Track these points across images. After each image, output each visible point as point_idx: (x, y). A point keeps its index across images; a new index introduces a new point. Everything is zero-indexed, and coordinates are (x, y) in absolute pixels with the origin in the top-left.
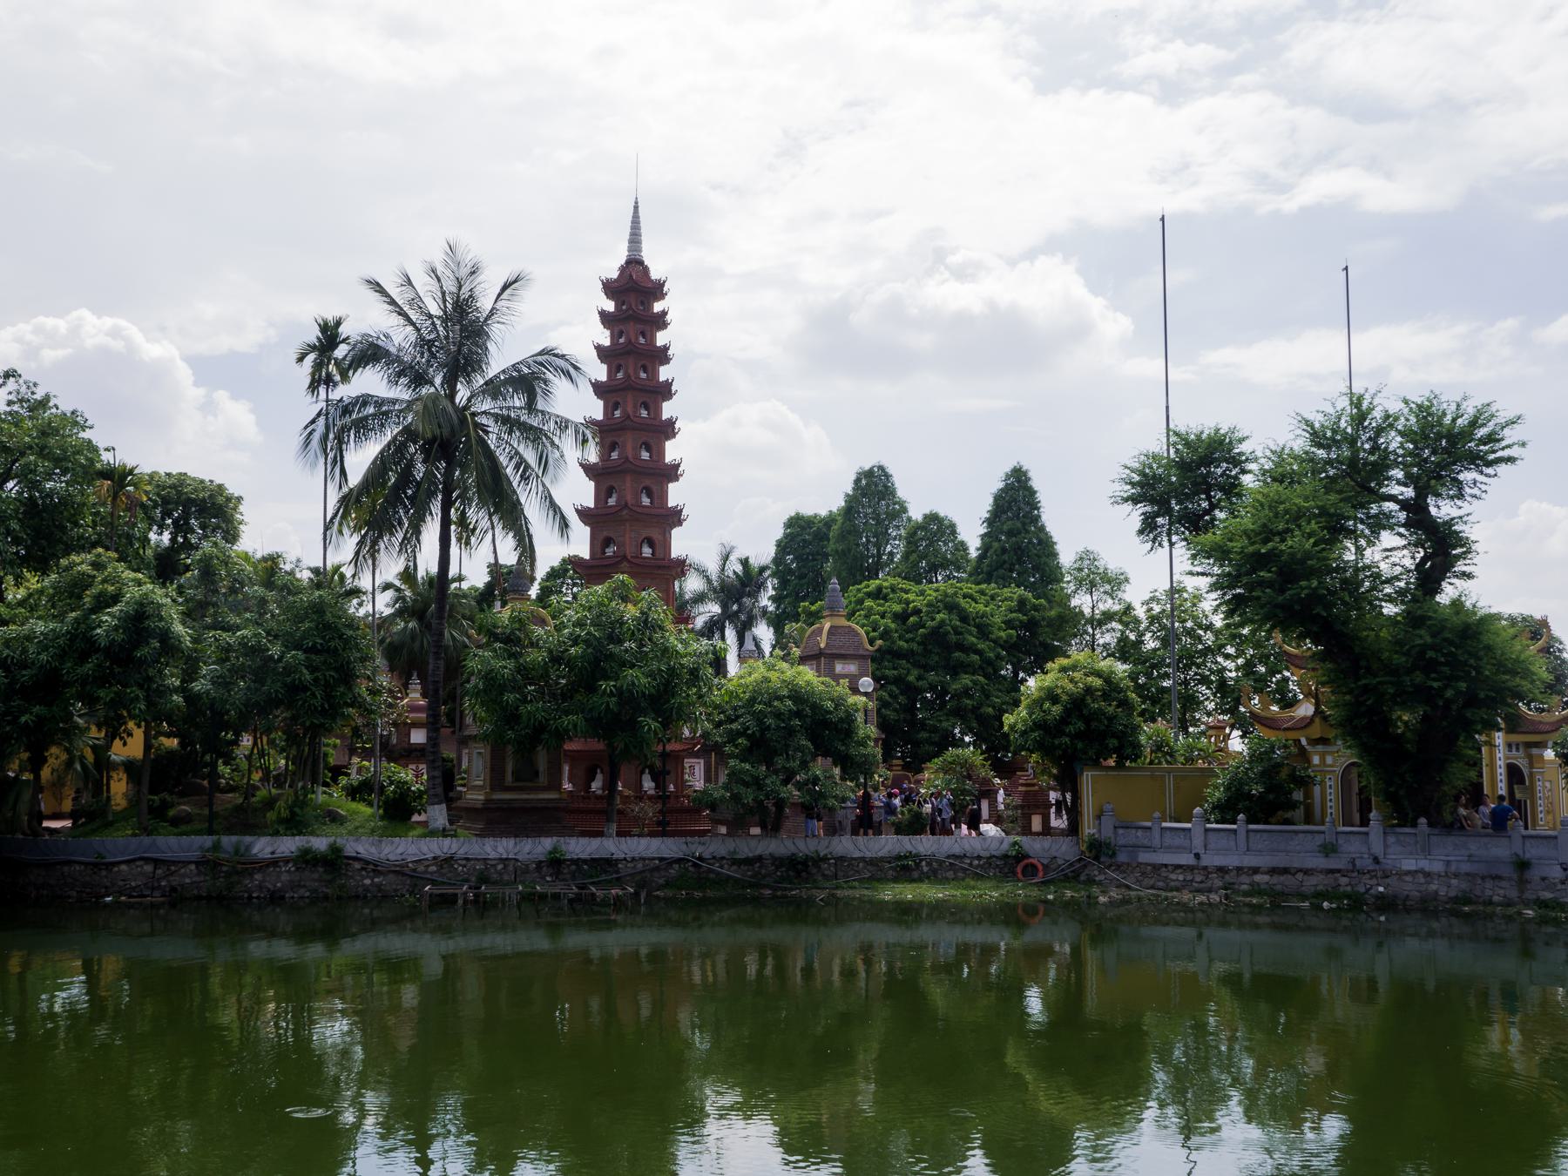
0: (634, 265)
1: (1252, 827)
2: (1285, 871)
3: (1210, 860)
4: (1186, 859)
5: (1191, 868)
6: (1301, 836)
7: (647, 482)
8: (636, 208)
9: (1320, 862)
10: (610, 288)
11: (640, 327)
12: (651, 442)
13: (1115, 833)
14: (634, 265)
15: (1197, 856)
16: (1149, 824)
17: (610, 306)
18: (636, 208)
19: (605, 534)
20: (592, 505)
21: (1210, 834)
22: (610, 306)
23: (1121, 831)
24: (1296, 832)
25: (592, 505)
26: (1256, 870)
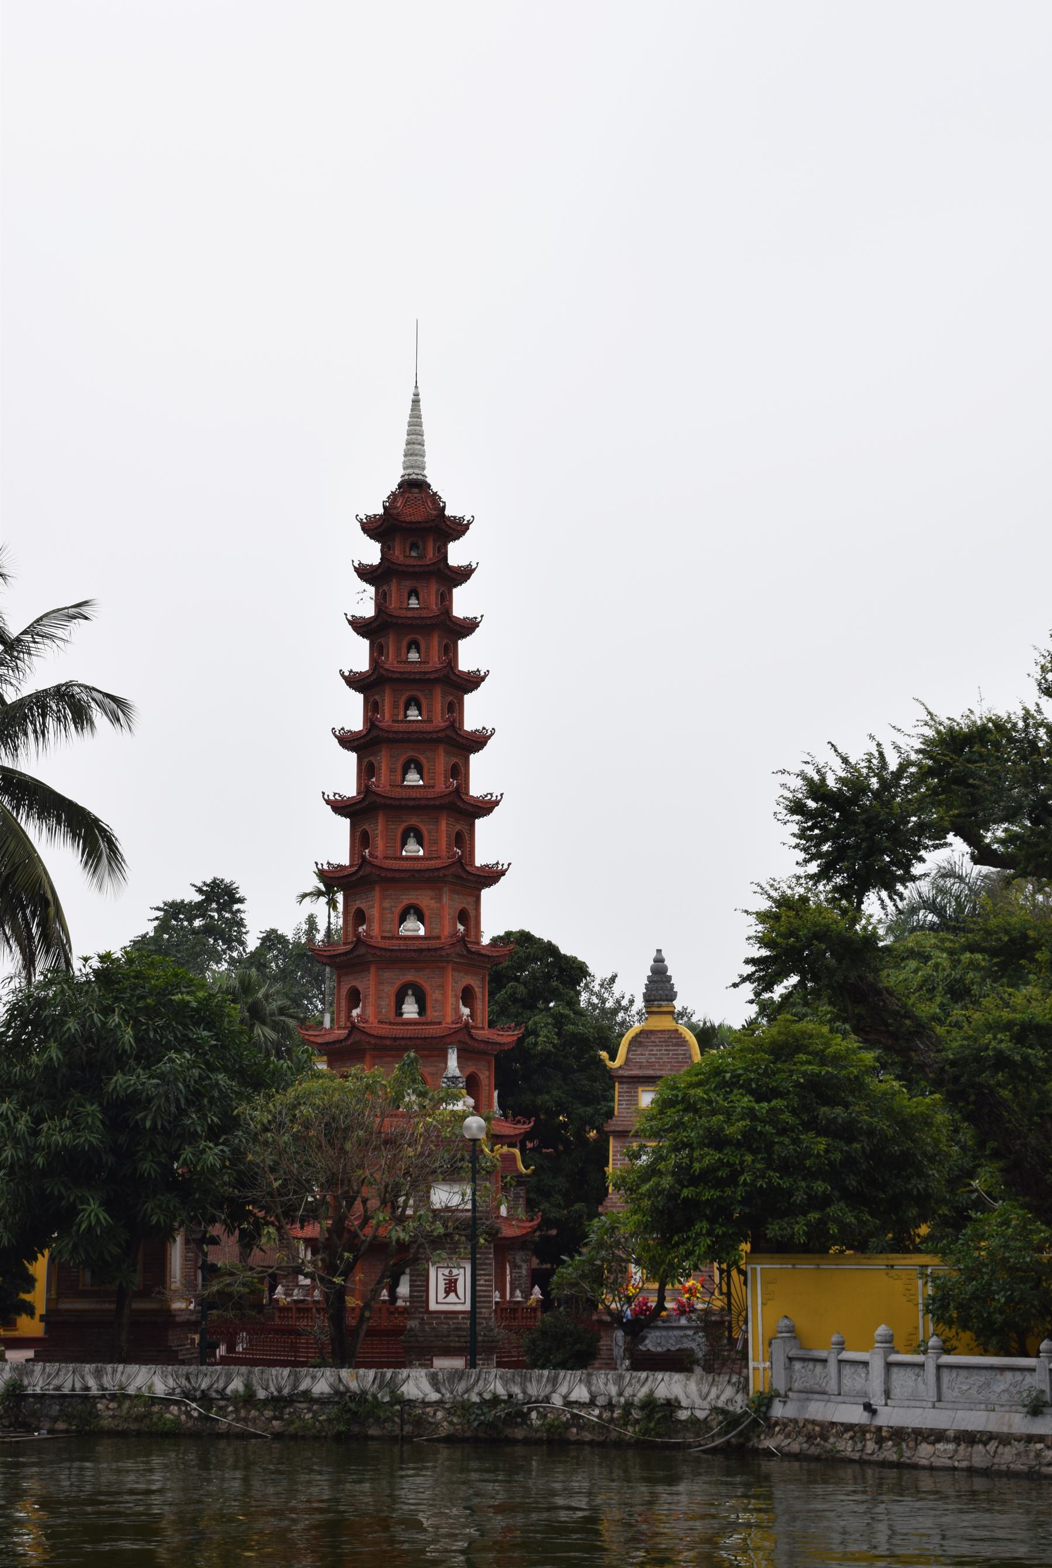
0: (414, 488)
1: (946, 1359)
2: (968, 1438)
3: (889, 1417)
4: (856, 1415)
5: (857, 1431)
6: (1009, 1375)
7: (414, 821)
8: (416, 402)
9: (1019, 1423)
10: (372, 528)
11: (408, 584)
12: (423, 759)
13: (789, 1368)
14: (414, 488)
15: (868, 1407)
16: (823, 1354)
17: (372, 553)
18: (416, 402)
19: (358, 904)
20: (346, 861)
21: (897, 1374)
22: (372, 553)
23: (798, 1365)
24: (1002, 1369)
25: (346, 861)
26: (937, 1436)
